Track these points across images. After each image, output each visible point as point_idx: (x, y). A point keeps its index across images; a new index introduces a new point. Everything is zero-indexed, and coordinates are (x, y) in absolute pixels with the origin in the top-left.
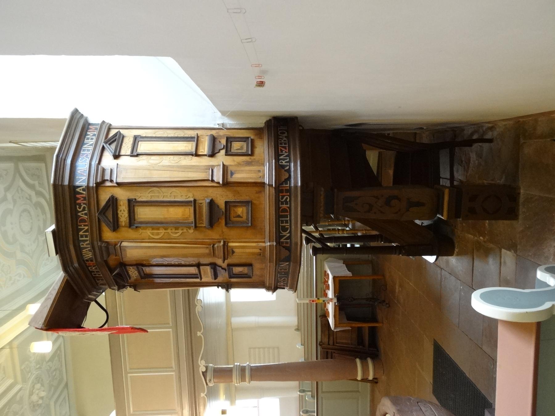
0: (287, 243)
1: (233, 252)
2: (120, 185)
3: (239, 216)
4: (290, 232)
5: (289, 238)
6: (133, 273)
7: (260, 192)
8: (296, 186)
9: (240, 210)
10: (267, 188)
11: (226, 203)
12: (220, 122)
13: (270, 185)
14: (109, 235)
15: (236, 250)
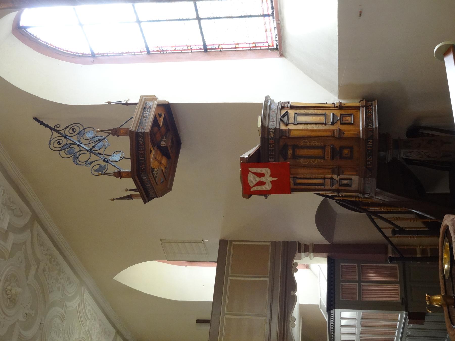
0: (371, 128)
1: (344, 133)
2: (292, 107)
3: (347, 120)
4: (373, 124)
5: (373, 126)
6: (290, 152)
7: (357, 112)
8: (376, 128)
9: (347, 118)
10: (361, 109)
11: (341, 114)
12: (338, 101)
13: (362, 107)
14: (283, 127)
15: (345, 132)
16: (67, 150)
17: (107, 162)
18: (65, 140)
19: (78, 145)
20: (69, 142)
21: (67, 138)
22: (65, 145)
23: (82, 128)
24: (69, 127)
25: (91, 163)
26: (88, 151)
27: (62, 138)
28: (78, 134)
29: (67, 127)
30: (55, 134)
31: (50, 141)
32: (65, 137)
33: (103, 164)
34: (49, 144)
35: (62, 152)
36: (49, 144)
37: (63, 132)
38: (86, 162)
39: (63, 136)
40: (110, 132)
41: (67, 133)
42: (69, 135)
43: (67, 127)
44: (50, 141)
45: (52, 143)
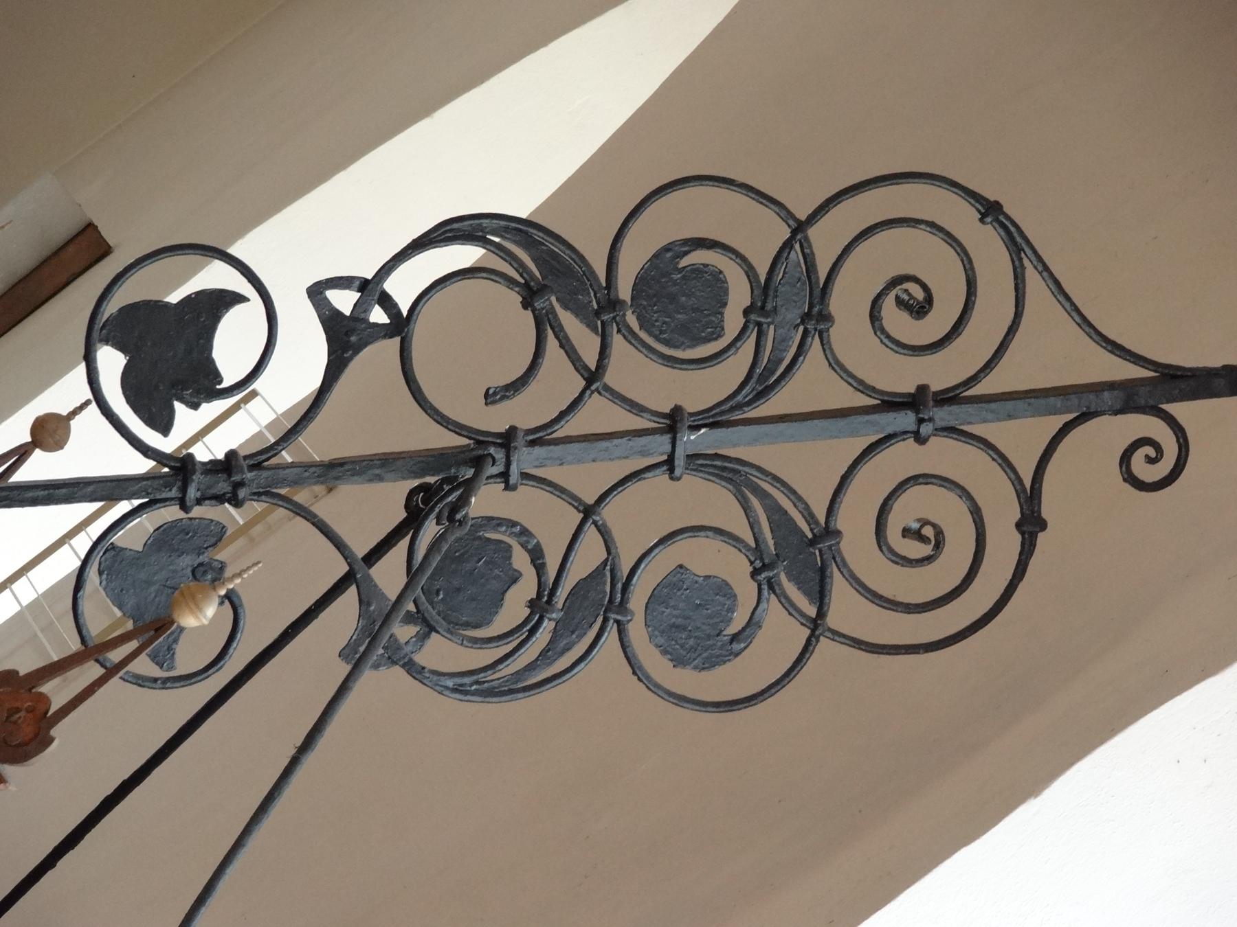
16: (739, 295)
17: (181, 467)
18: (902, 376)
19: (673, 422)
20: (812, 385)
21: (891, 403)
22: (817, 317)
23: (845, 608)
24: (1004, 544)
25: (344, 338)
26: (507, 439)
27: (940, 372)
28: (829, 532)
29: (1031, 524)
30: (1053, 354)
31: (1017, 243)
32: (916, 401)
33: (207, 432)
34: (991, 210)
35: (761, 238)
36: (991, 210)
37: (1023, 437)
38: (400, 325)
39: (949, 397)
40: (57, 692)
41: (943, 455)
42: (903, 458)
43: (1031, 524)
44: (1017, 243)
45: (988, 246)
